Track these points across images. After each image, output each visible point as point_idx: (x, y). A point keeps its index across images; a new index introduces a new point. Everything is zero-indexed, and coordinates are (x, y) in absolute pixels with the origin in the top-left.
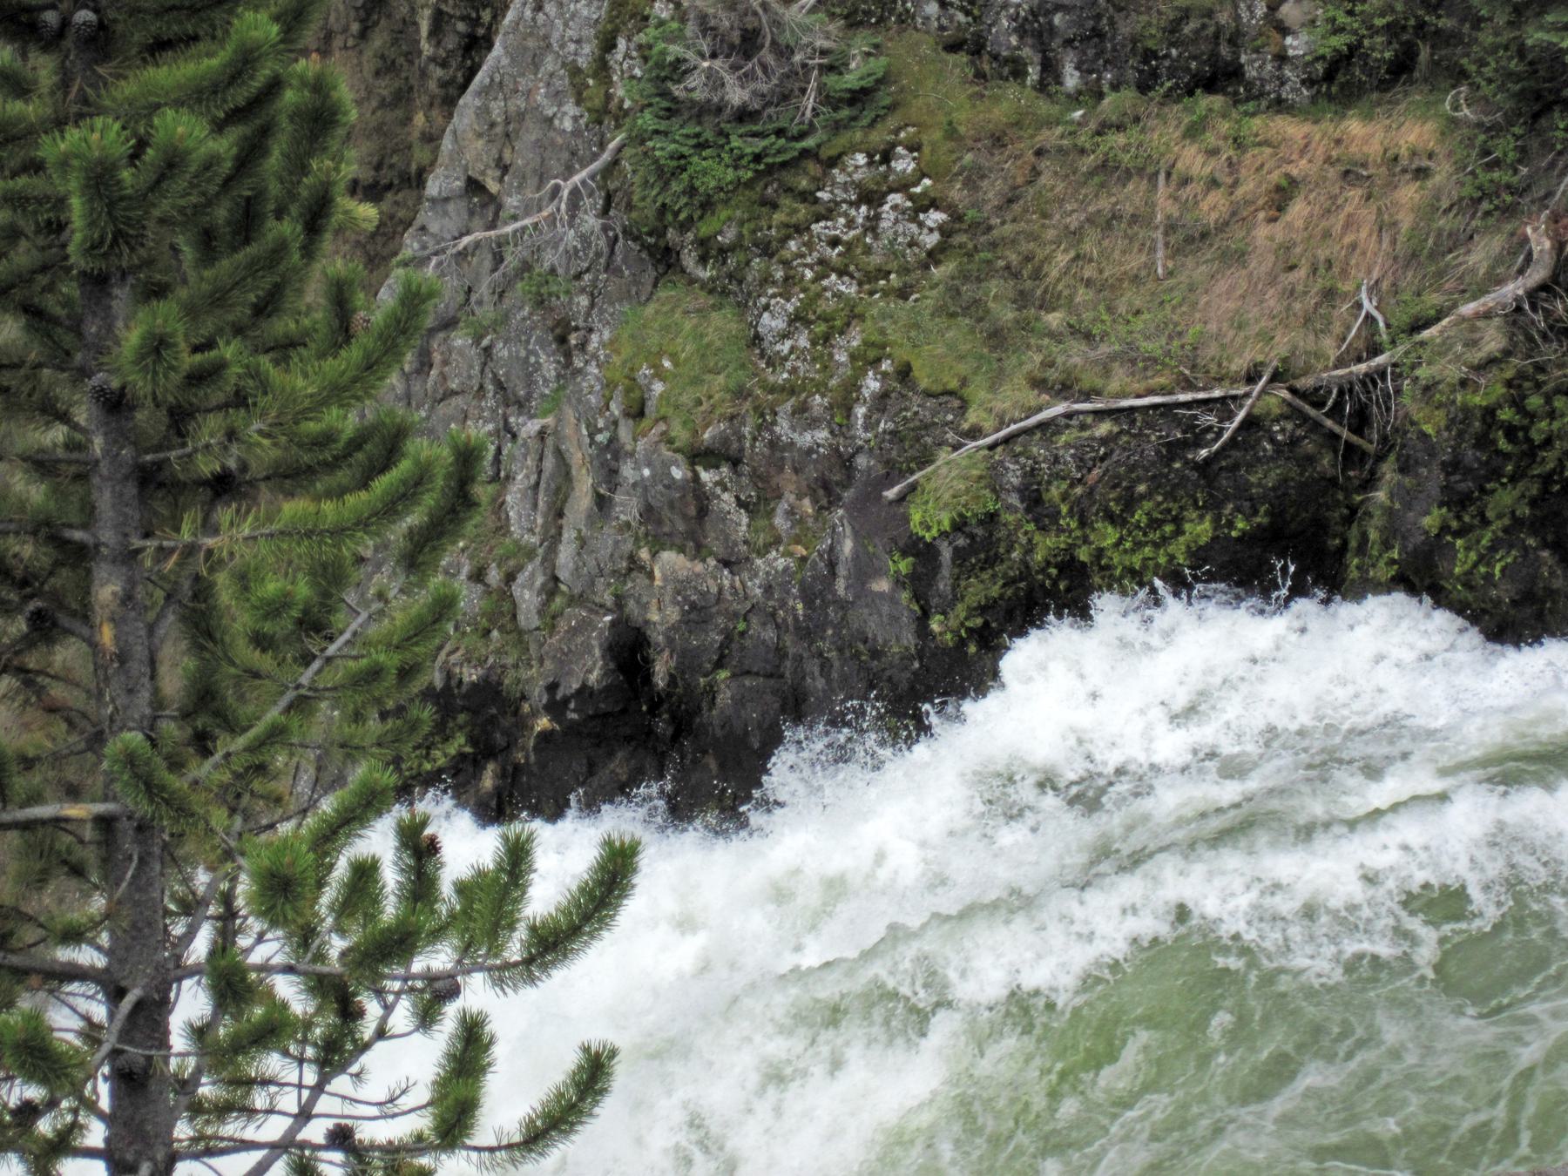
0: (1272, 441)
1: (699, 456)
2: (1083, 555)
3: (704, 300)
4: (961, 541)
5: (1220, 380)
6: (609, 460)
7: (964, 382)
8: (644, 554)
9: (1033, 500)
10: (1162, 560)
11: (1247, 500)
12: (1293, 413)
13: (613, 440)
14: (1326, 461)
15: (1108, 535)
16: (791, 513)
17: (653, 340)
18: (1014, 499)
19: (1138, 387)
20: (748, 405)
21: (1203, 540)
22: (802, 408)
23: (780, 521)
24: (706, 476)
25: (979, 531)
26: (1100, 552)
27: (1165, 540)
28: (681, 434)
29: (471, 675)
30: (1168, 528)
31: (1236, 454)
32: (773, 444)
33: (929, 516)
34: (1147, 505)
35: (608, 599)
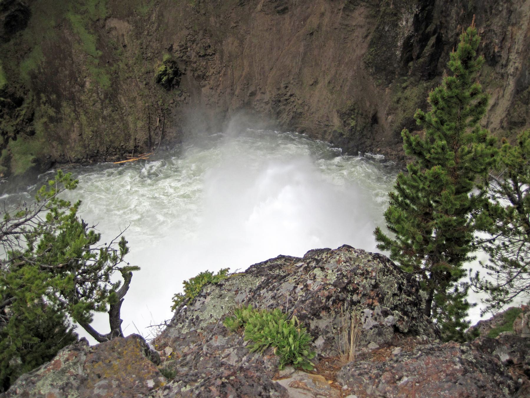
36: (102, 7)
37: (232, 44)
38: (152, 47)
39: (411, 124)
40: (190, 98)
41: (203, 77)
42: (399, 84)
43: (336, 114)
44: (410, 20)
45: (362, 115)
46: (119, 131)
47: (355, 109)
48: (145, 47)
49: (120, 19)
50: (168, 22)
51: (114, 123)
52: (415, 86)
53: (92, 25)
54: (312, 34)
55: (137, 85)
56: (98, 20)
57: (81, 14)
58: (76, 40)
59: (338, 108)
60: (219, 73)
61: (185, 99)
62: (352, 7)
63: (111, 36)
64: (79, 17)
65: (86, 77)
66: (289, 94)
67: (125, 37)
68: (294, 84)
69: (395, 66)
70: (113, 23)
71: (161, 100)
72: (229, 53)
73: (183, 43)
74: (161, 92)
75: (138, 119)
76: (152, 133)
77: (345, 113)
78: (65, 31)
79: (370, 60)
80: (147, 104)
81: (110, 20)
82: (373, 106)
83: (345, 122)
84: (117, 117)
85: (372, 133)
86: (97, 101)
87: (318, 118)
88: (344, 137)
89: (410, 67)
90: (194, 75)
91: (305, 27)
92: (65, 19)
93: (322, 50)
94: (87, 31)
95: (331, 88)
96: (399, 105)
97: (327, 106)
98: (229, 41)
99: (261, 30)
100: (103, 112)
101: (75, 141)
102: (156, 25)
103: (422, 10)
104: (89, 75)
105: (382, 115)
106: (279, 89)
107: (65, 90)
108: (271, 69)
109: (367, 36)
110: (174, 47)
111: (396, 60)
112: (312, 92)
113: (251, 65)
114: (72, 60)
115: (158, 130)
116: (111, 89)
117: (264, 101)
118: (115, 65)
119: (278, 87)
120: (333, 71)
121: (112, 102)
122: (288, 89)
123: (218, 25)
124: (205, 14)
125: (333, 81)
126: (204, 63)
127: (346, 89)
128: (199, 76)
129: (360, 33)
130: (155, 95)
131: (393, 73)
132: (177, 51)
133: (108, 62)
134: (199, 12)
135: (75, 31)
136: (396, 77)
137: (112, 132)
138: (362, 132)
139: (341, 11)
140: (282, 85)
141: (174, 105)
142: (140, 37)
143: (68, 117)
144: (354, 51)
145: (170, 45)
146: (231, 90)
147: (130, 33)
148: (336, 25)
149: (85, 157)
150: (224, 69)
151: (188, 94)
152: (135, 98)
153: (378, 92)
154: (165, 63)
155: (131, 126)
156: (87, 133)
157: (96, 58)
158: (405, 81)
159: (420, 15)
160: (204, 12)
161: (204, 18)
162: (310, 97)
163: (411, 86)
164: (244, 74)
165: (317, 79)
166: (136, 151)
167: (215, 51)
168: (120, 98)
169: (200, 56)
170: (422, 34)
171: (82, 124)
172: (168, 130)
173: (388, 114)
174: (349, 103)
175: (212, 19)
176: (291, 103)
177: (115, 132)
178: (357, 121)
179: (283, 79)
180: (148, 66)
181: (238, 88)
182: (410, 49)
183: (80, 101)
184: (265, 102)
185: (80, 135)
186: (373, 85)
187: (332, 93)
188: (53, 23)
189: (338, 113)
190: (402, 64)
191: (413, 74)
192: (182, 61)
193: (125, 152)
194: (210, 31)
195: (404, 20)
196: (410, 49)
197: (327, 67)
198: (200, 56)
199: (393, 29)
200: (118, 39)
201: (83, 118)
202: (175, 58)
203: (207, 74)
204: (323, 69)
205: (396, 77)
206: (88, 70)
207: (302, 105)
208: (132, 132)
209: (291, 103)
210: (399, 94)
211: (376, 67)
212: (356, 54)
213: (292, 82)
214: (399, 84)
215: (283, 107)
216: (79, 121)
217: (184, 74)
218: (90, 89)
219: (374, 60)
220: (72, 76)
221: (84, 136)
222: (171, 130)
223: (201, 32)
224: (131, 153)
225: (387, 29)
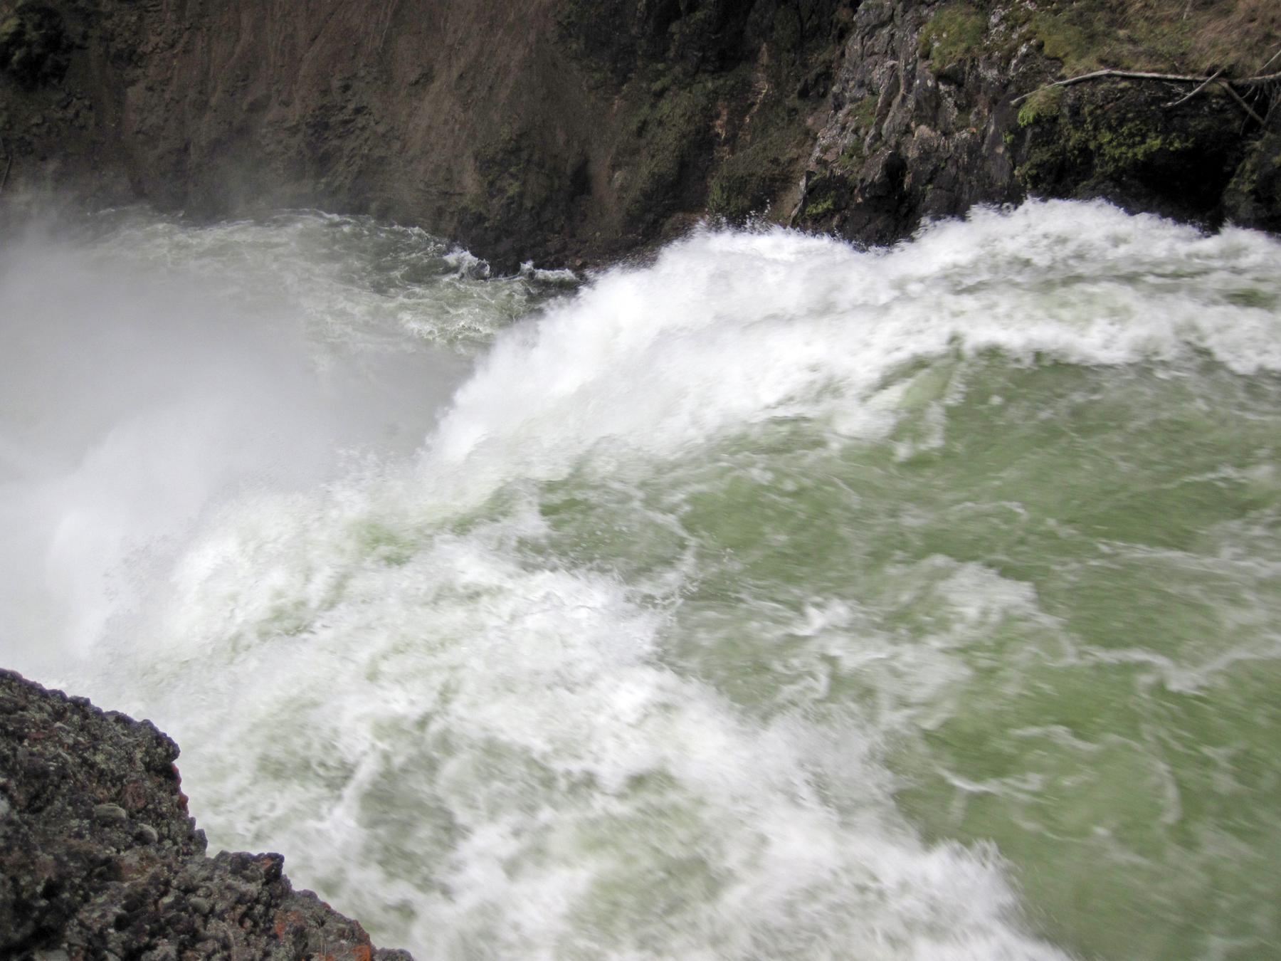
0: (1210, 107)
1: (941, 77)
2: (1092, 145)
3: (973, 9)
4: (1038, 130)
5: (1193, 72)
6: (911, 76)
7: (1066, 55)
8: (913, 125)
9: (1075, 111)
10: (1130, 155)
11: (1185, 133)
12: (1226, 95)
13: (914, 69)
14: (1236, 124)
15: (1106, 137)
16: (978, 113)
17: (943, 23)
18: (1066, 111)
19: (1149, 67)
20: (968, 56)
21: (1155, 149)
22: (990, 57)
23: (972, 117)
24: (942, 87)
25: (1047, 126)
26: (1100, 146)
27: (1134, 145)
28: (937, 65)
29: (838, 172)
30: (1138, 139)
31: (1188, 109)
32: (977, 77)
33: (1026, 115)
34: (1130, 125)
35: (893, 142)
41: (131, 57)
43: (472, 161)
45: (541, 165)
47: (519, 149)
60: (172, 46)
61: (77, 115)
66: (351, 106)
68: (369, 79)
77: (493, 160)
79: (573, 18)
82: (576, 144)
83: (491, 184)
88: (487, 225)
89: (672, 34)
90: (107, 52)
96: (643, 142)
105: (600, 168)
111: (635, 15)
117: (287, 125)
119: (323, 88)
122: (350, 92)
126: (134, 19)
127: (503, 95)
128: (119, 56)
136: (639, 63)
138: (538, 214)
140: (336, 83)
141: (44, 129)
150: (186, 35)
151: (87, 103)
158: (659, 75)
162: (410, 115)
163: (674, 88)
164: (238, 50)
165: (431, 69)
173: (615, 167)
174: (505, 132)
176: (357, 132)
178: (524, 183)
181: (220, 88)
184: (289, 129)
190: (649, 29)
191: (681, 57)
203: (140, 50)
204: (448, 41)
205: (639, 63)
209: (357, 132)
210: (645, 110)
213: (362, 73)
214: (644, 85)
215: (336, 142)
217: (80, 47)
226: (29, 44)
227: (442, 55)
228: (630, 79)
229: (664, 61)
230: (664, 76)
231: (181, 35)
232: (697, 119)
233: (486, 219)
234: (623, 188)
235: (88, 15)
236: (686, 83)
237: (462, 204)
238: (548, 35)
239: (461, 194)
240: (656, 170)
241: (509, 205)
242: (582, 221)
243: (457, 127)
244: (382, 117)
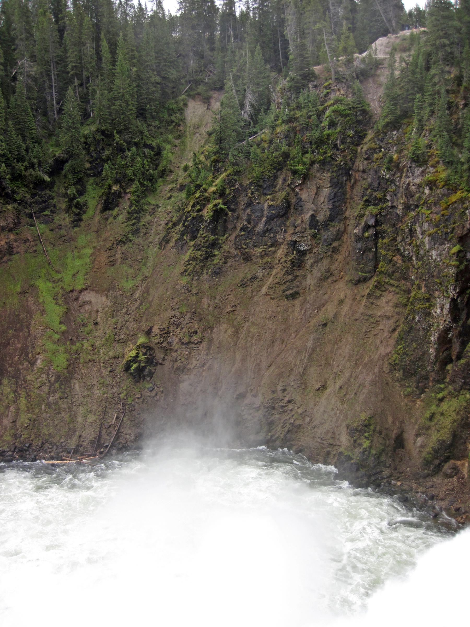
36: (80, 277)
37: (225, 332)
38: (127, 328)
39: (446, 450)
40: (163, 395)
42: (433, 395)
43: (345, 429)
44: (445, 307)
45: (380, 433)
46: (62, 424)
47: (370, 425)
48: (120, 327)
49: (98, 292)
50: (152, 300)
51: (58, 413)
52: (455, 397)
53: (63, 295)
54: (325, 325)
55: (99, 371)
56: (72, 291)
57: (54, 282)
58: (40, 310)
59: (349, 421)
60: (203, 366)
61: (156, 394)
62: (378, 292)
63: (83, 311)
64: (50, 285)
65: (39, 353)
66: (286, 399)
67: (99, 314)
68: (295, 386)
69: (428, 369)
70: (89, 296)
71: (125, 392)
72: (219, 343)
73: (164, 326)
74: (127, 382)
75: (90, 412)
76: (104, 432)
77: (356, 429)
78: (30, 299)
79: (397, 361)
80: (105, 395)
81: (86, 292)
82: (397, 423)
83: (355, 441)
84: (65, 406)
85: (393, 460)
86: (45, 384)
87: (321, 434)
88: (352, 461)
90: (172, 367)
91: (317, 317)
92: (32, 286)
93: (336, 346)
94: (54, 301)
95: (342, 395)
96: (433, 423)
97: (334, 419)
98: (222, 328)
99: (263, 318)
100: (48, 398)
101: (6, 429)
102: (138, 303)
103: (461, 293)
104: (44, 351)
105: (409, 435)
106: (274, 392)
107: (11, 365)
108: (269, 367)
109: (394, 330)
110: (153, 330)
112: (317, 399)
113: (243, 360)
114: (29, 332)
115: (111, 429)
116: (66, 371)
118: (78, 344)
120: (347, 374)
121: (63, 387)
122: (286, 392)
123: (211, 308)
124: (196, 294)
125: (346, 386)
126: (187, 353)
127: (362, 397)
128: (178, 369)
129: (386, 325)
130: (119, 386)
131: (426, 378)
132: (156, 335)
133: (71, 340)
134: (190, 291)
135: (41, 300)
136: (430, 384)
137: (53, 423)
138: (378, 458)
139: (365, 299)
140: (280, 388)
142: (117, 316)
143: (5, 397)
144: (377, 348)
145: (149, 328)
146: (214, 388)
147: (106, 309)
148: (358, 315)
149: (13, 449)
150: (210, 362)
151: (161, 389)
152: (93, 386)
153: (407, 405)
154: (138, 347)
155: (80, 419)
156: (22, 420)
157: (57, 333)
158: (442, 390)
159: (459, 300)
160: (196, 292)
161: (194, 298)
162: (315, 405)
163: (449, 397)
165: (326, 383)
166: (77, 452)
167: (202, 338)
168: (75, 384)
169: (183, 343)
170: (462, 326)
171: (19, 409)
172: (125, 431)
173: (418, 435)
174: (363, 416)
175: (205, 301)
176: (289, 412)
177: (57, 425)
178: (372, 442)
179: (281, 380)
180: (118, 349)
182: (448, 346)
183: (25, 381)
184: (255, 408)
185: (13, 422)
186: (400, 395)
187: (343, 402)
188: (18, 289)
189: (348, 428)
190: (437, 367)
191: (453, 381)
192: (161, 347)
193: (63, 451)
194: (200, 314)
195: (438, 307)
196: (448, 346)
197: (340, 367)
198: (183, 343)
199: (425, 319)
200: (90, 314)
201: (23, 401)
202: (154, 344)
203: (188, 367)
204: (335, 370)
205: (430, 384)
206: (43, 346)
207: (303, 416)
208: (78, 426)
209: (289, 412)
210: (433, 408)
211: (404, 370)
212: (379, 353)
214: (433, 395)
215: (277, 416)
216: (17, 405)
217: (161, 364)
218: (40, 368)
219: (401, 361)
220: (24, 351)
221: (18, 424)
222: (129, 431)
223: (189, 315)
224: (69, 453)
225: (417, 319)
226: (140, 361)
227: (332, 377)
228: (425, 392)
229: (443, 383)
230: (444, 390)
231: (208, 361)
232: (461, 413)
233: (352, 459)
234: (422, 446)
235: (167, 350)
236: (455, 394)
237: (340, 451)
238: (384, 369)
239: (339, 446)
240: (441, 438)
241: (364, 452)
242: (400, 462)
243: (338, 412)
244: (301, 405)
